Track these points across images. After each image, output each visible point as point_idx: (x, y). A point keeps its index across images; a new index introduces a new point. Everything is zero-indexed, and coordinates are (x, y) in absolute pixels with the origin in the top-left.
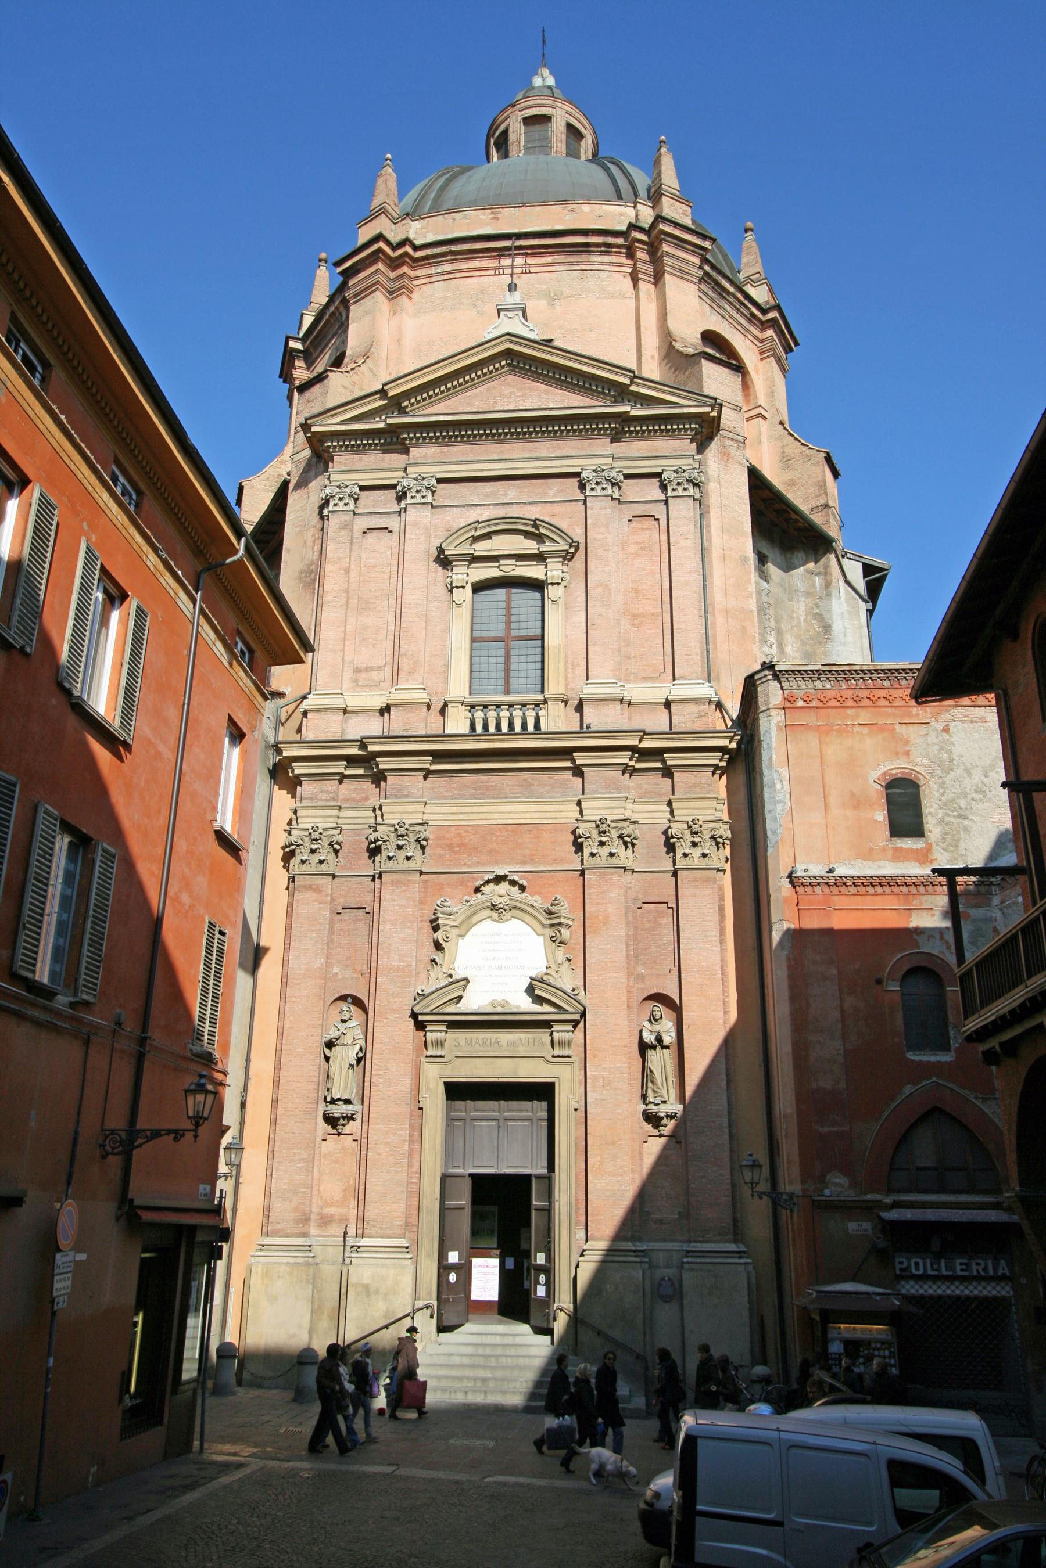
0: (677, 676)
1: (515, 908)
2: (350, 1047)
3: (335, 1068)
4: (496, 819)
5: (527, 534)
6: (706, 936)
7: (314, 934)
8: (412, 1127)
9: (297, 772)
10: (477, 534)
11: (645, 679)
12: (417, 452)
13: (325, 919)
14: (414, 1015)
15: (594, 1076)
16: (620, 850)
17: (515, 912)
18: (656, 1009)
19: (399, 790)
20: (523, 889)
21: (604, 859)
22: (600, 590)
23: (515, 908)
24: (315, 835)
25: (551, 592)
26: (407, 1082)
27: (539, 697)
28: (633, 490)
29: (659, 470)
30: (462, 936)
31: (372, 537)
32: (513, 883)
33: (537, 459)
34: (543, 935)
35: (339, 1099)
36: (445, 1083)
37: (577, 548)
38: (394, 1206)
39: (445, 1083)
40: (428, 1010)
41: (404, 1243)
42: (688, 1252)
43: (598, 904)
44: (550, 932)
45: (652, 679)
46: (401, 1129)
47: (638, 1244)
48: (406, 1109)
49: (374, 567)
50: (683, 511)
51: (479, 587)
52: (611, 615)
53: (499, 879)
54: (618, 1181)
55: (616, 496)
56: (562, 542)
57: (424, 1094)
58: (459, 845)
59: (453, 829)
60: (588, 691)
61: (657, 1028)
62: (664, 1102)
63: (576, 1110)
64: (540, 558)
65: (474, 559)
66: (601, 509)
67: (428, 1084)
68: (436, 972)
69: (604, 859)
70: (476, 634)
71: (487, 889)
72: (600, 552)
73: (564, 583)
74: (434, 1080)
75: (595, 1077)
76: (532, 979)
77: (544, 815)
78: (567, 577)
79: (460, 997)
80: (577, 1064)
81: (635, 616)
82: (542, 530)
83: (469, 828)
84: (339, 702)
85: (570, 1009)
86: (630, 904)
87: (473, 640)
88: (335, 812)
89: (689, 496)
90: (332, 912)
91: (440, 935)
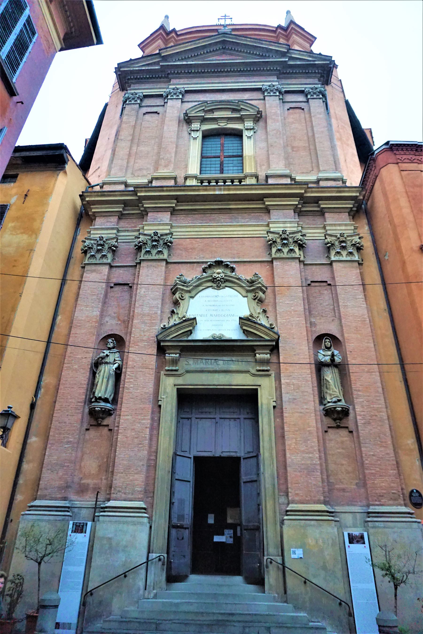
0: (321, 169)
1: (227, 281)
2: (112, 365)
3: (99, 378)
4: (215, 234)
5: (234, 110)
6: (356, 299)
7: (95, 297)
8: (152, 419)
9: (93, 210)
10: (206, 109)
11: (303, 173)
12: (173, 81)
13: (102, 288)
14: (159, 342)
15: (286, 383)
16: (297, 249)
17: (228, 284)
18: (328, 340)
19: (155, 219)
20: (233, 270)
21: (285, 253)
22: (275, 132)
23: (227, 281)
24: (102, 242)
25: (246, 134)
26: (150, 388)
27: (242, 175)
28: (289, 98)
29: (304, 89)
30: (192, 297)
31: (147, 117)
32: (227, 266)
33: (238, 82)
34: (247, 297)
35: (100, 398)
36: (177, 389)
37: (261, 116)
38: (136, 476)
39: (178, 389)
40: (168, 338)
41: (142, 504)
42: (369, 513)
43: (283, 278)
44: (251, 295)
45: (307, 173)
46: (144, 419)
47: (329, 507)
48: (149, 406)
49: (148, 127)
50: (316, 105)
51: (207, 136)
52: (282, 142)
53: (219, 263)
54: (310, 458)
55: (281, 97)
56: (252, 111)
57: (162, 396)
58: (191, 249)
59: (188, 240)
60: (270, 172)
61: (330, 353)
62: (339, 401)
63: (274, 407)
64: (241, 119)
65: (204, 120)
66: (274, 101)
67: (165, 389)
68: (175, 317)
69: (285, 253)
70: (204, 155)
71: (209, 272)
72: (273, 117)
73: (255, 131)
74: (169, 386)
75: (288, 384)
76: (240, 318)
77: (246, 233)
78: (256, 128)
79: (191, 332)
80: (273, 375)
81: (293, 147)
82: (242, 107)
83: (198, 240)
84: (123, 179)
85: (267, 338)
86: (304, 280)
87: (202, 157)
88: (115, 231)
89: (320, 98)
90: (107, 286)
91: (177, 295)
